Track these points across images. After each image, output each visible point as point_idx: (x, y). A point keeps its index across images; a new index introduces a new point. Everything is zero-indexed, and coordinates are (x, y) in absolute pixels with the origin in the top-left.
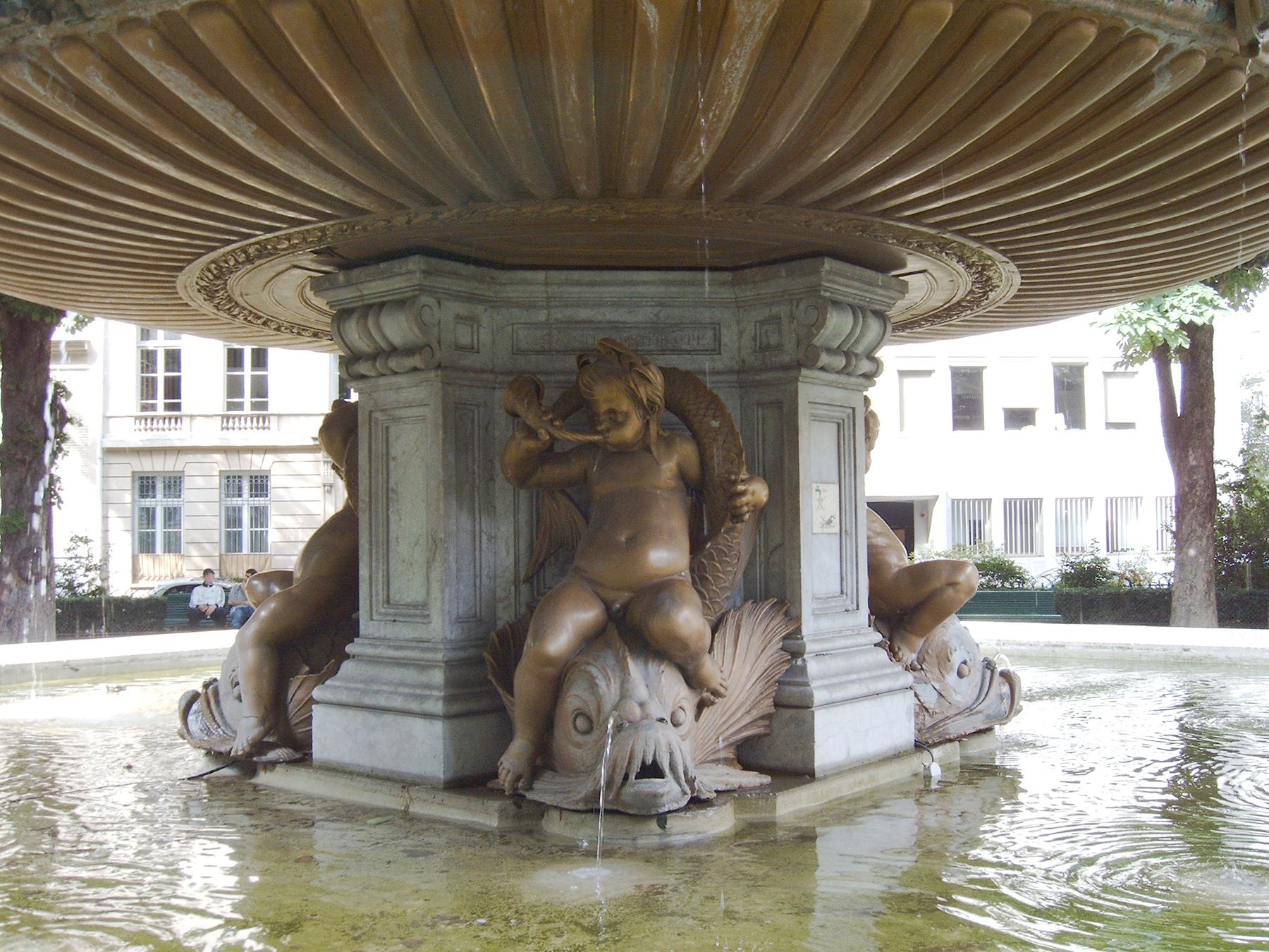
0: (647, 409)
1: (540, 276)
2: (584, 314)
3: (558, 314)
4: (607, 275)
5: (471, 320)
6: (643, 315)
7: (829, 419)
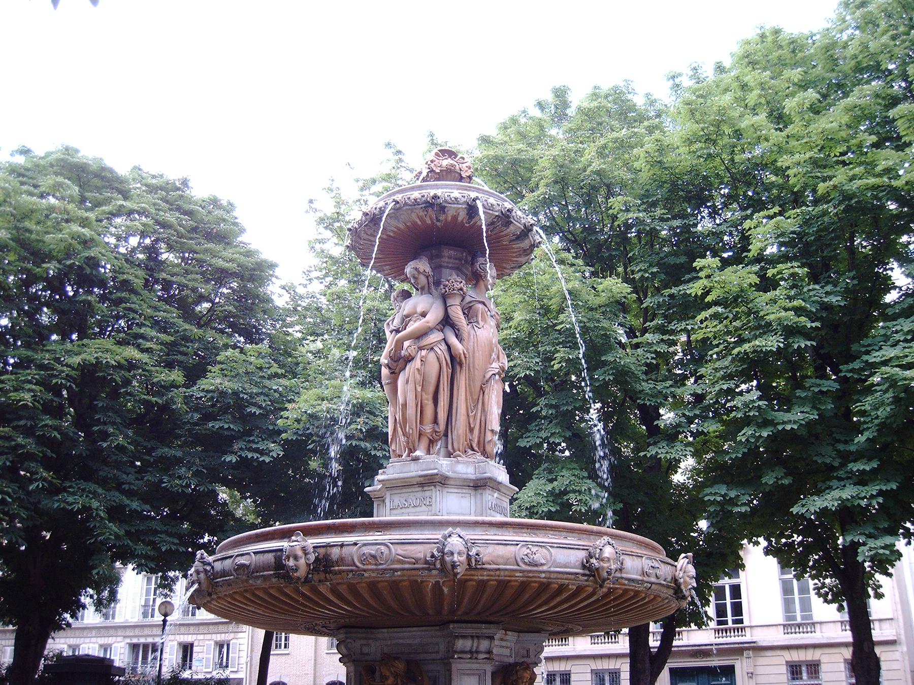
0: (396, 675)
1: (385, 630)
2: (401, 641)
3: (394, 642)
4: (404, 629)
5: (367, 645)
6: (417, 641)
7: (473, 674)
